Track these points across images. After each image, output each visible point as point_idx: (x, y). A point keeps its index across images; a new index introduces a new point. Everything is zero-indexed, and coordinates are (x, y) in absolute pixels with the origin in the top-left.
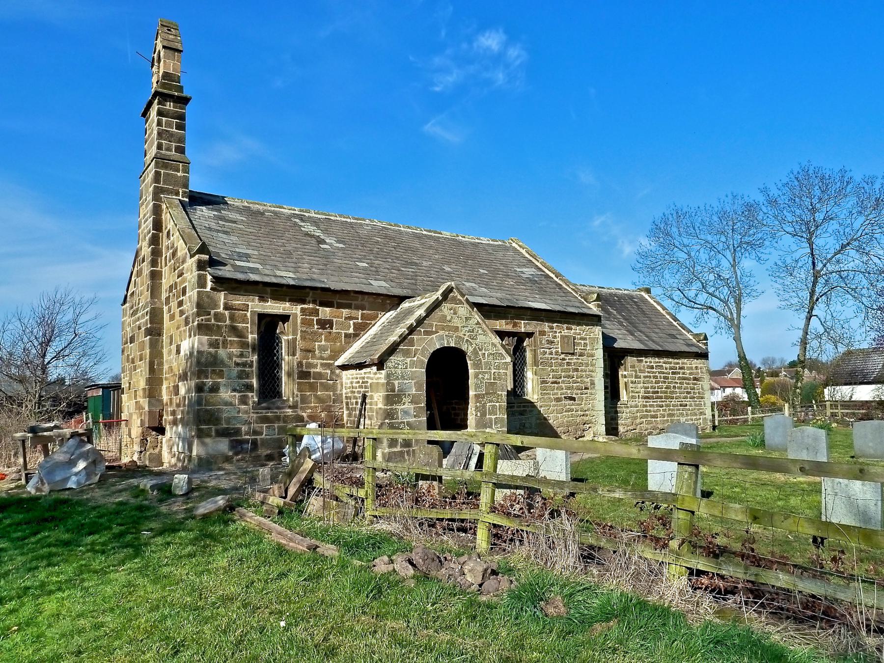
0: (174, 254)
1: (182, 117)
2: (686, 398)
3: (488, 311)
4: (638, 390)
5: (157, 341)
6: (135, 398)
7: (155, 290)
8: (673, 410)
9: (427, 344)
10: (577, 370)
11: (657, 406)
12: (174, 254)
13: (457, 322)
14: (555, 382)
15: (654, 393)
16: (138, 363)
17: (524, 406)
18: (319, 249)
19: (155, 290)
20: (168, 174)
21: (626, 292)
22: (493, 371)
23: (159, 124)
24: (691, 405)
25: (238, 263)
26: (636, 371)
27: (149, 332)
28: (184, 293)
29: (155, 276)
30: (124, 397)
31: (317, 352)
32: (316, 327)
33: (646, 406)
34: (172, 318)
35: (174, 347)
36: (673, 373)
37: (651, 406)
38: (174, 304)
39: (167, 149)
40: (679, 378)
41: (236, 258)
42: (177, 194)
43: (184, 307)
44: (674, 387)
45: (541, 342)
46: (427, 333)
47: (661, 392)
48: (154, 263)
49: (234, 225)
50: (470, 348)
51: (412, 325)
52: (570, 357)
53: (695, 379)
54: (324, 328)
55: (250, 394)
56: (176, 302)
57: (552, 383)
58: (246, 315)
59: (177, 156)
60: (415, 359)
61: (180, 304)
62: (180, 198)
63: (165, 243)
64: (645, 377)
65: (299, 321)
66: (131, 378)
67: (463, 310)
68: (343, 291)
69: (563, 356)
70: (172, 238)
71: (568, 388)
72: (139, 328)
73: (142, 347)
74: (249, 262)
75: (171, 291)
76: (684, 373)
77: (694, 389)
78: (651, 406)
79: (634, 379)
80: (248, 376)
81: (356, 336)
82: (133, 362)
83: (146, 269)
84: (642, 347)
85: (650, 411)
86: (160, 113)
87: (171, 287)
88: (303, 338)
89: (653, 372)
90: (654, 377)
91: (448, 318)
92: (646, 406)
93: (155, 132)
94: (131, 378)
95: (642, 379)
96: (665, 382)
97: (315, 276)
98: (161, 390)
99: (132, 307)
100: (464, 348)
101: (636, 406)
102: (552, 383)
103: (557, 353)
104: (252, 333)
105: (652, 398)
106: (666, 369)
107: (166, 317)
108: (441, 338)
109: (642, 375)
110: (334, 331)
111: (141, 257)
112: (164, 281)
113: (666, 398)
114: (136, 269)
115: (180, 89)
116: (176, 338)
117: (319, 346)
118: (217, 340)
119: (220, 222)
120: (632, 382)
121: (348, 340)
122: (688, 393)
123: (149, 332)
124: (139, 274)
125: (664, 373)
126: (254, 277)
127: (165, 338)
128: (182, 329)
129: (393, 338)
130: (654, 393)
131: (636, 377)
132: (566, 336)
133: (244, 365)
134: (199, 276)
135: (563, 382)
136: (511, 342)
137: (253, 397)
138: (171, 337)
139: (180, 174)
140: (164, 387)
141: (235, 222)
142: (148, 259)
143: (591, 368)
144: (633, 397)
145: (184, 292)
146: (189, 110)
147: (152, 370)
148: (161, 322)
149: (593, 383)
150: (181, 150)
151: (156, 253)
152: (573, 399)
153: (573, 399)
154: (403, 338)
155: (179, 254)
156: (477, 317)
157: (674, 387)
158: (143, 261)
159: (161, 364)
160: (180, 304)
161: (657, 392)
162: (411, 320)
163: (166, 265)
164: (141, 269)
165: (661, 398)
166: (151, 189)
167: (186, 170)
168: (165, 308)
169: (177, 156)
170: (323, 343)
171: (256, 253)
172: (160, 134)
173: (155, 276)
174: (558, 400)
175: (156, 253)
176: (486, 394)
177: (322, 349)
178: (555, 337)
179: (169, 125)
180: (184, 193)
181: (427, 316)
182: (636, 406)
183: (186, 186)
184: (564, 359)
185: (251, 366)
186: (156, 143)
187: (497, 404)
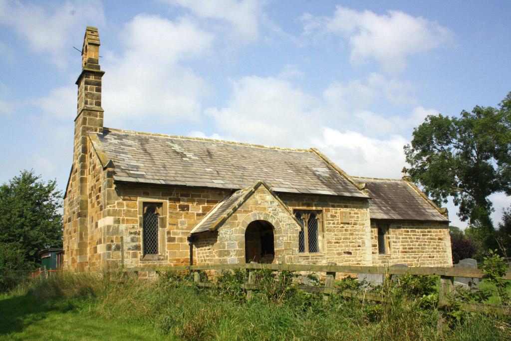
0: (94, 167)
1: (99, 84)
2: (433, 252)
3: (285, 197)
4: (397, 247)
5: (84, 220)
6: (72, 256)
7: (82, 190)
8: (424, 260)
9: (244, 219)
10: (352, 234)
11: (413, 257)
12: (94, 167)
13: (266, 205)
14: (337, 243)
15: (410, 249)
16: (73, 234)
17: (316, 259)
18: (182, 161)
19: (82, 190)
20: (91, 119)
21: (393, 181)
22: (289, 235)
23: (86, 89)
24: (437, 257)
25: (132, 172)
26: (396, 235)
27: (79, 215)
28: (100, 191)
29: (82, 180)
30: (65, 256)
31: (179, 225)
32: (178, 209)
33: (404, 258)
34: (93, 206)
35: (94, 224)
36: (423, 235)
37: (407, 257)
38: (94, 198)
39: (91, 104)
40: (428, 239)
41: (130, 169)
42: (96, 130)
43: (100, 200)
44: (424, 245)
45: (327, 216)
46: (246, 212)
47: (415, 248)
48: (82, 173)
49: (131, 148)
50: (274, 221)
51: (235, 207)
52: (347, 225)
53: (440, 239)
54: (183, 210)
55: (138, 252)
56: (95, 197)
57: (335, 243)
58: (136, 203)
59: (97, 108)
60: (238, 228)
61: (98, 197)
62: (98, 132)
63: (88, 161)
64: (403, 238)
65: (168, 206)
66: (69, 243)
67: (269, 197)
68: (216, 188)
69: (342, 225)
70: (93, 157)
71: (347, 246)
72: (74, 213)
73: (75, 225)
74: (138, 171)
75: (92, 190)
76: (431, 235)
77: (438, 246)
78: (407, 257)
79: (395, 240)
80: (138, 240)
81: (204, 214)
82: (70, 234)
83: (78, 176)
84: (399, 217)
85: (407, 261)
86: (86, 83)
87: (92, 187)
88: (171, 217)
89: (408, 235)
90: (410, 238)
91: (259, 202)
92: (404, 258)
93: (84, 94)
94: (69, 243)
95: (401, 240)
96: (417, 241)
97: (177, 178)
98: (86, 251)
99: (70, 200)
100: (270, 220)
101: (397, 258)
102: (335, 243)
103: (338, 224)
104: (139, 214)
105: (409, 252)
106: (418, 232)
107: (89, 205)
108: (255, 215)
109: (401, 237)
110: (190, 211)
111: (74, 170)
112: (88, 183)
113: (419, 252)
114: (72, 176)
115: (99, 67)
116: (95, 218)
117: (181, 222)
118: (119, 219)
119: (122, 147)
120: (394, 242)
121: (198, 217)
122: (434, 248)
123: (79, 215)
124: (74, 180)
125: (416, 235)
126: (141, 180)
127: (89, 219)
128: (98, 213)
129: (225, 215)
130: (410, 249)
131: (396, 238)
132: (344, 212)
133: (135, 233)
134: (108, 181)
135: (343, 242)
136: (306, 217)
137: (140, 253)
138: (93, 217)
139: (98, 118)
140: (88, 248)
141: (131, 146)
142: (79, 171)
143: (362, 233)
144: (395, 252)
145: (100, 190)
146: (104, 79)
147: (81, 237)
148: (87, 208)
149: (363, 243)
150: (99, 104)
151: (83, 167)
152: (350, 253)
153: (350, 253)
154: (229, 215)
155: (97, 167)
156: (277, 202)
157: (424, 245)
158: (76, 172)
159: (86, 234)
160: (98, 197)
161: (412, 248)
162: (236, 204)
163: (89, 174)
164: (75, 177)
165: (415, 252)
166: (81, 128)
167: (102, 116)
168: (89, 200)
169: (97, 108)
170: (183, 219)
171: (143, 165)
172: (86, 95)
173: (82, 180)
174: (339, 254)
175: (83, 167)
176: (285, 249)
177: (182, 223)
178: (336, 213)
179: (91, 89)
180: (100, 129)
181: (244, 201)
182: (397, 258)
183: (101, 125)
184: (343, 227)
185: (139, 234)
186: (84, 101)
187: (293, 256)
